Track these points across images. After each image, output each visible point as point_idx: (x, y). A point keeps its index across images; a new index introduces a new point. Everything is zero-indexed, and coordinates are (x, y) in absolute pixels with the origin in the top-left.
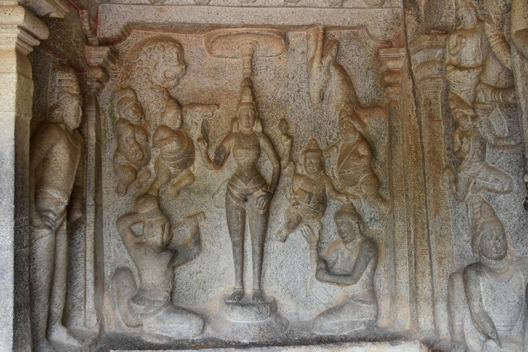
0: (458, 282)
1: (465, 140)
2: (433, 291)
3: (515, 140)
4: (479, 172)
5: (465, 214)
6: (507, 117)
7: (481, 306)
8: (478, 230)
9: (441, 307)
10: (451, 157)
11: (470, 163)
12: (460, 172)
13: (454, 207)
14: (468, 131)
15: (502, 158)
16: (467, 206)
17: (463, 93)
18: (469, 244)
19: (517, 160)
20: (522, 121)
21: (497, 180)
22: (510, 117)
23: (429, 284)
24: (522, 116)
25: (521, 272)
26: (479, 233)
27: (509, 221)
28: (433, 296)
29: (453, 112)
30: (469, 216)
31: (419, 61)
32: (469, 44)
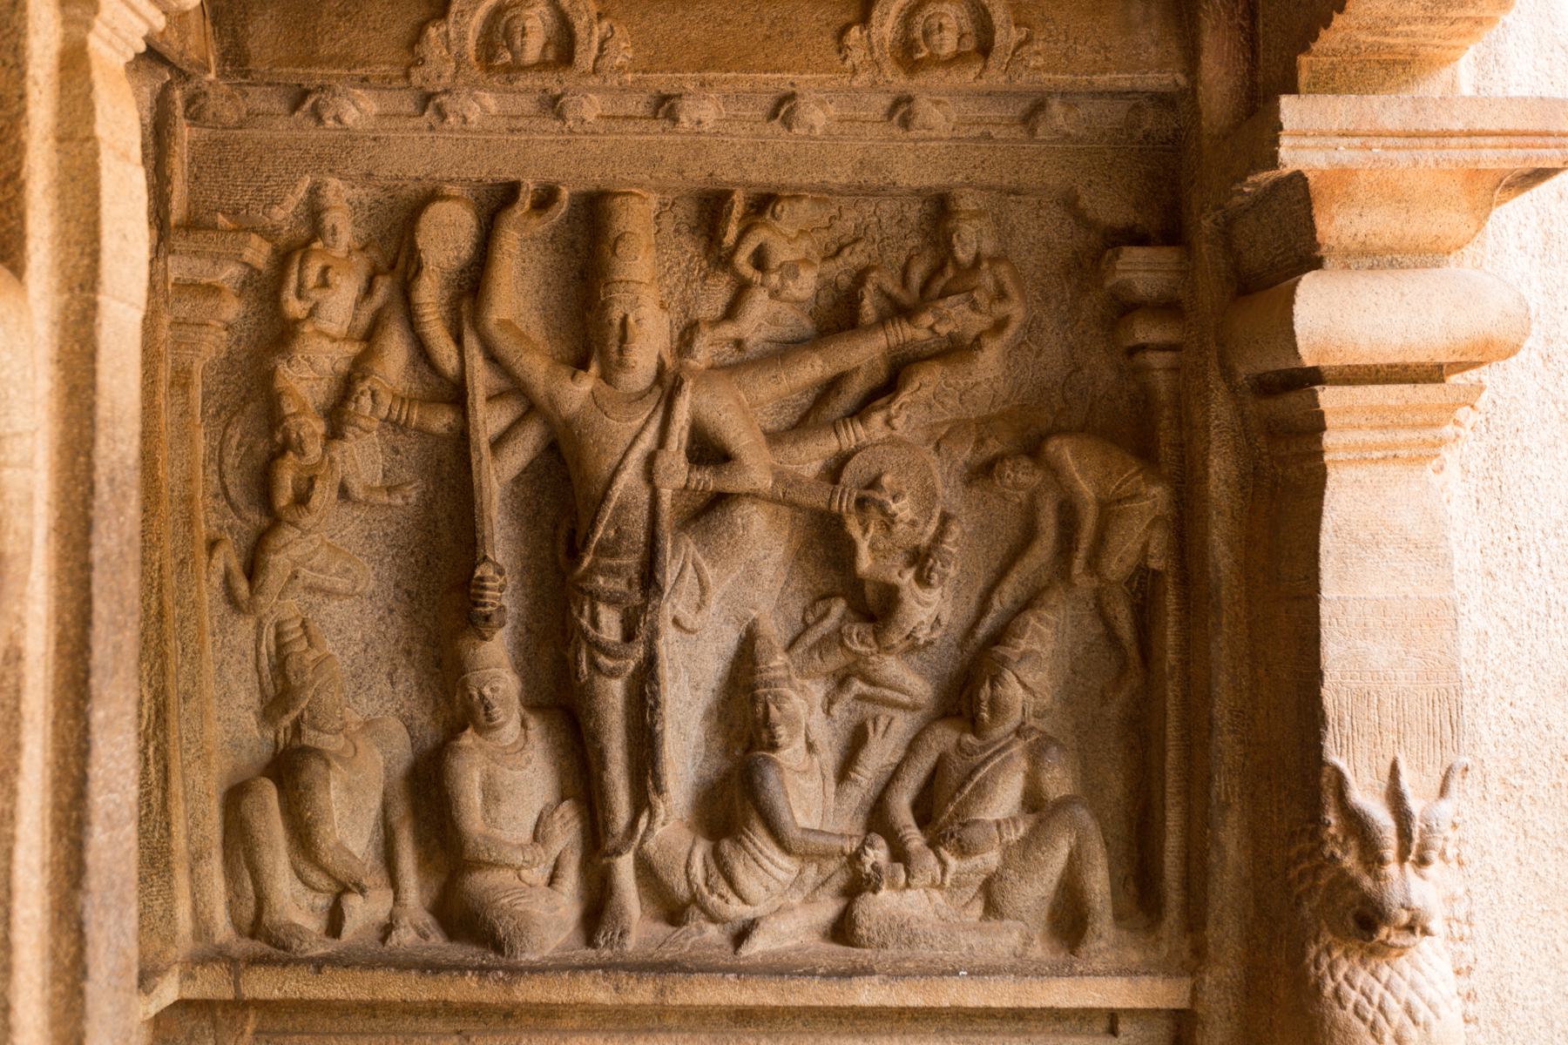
0: (269, 794)
1: (318, 485)
2: (189, 838)
3: (404, 497)
4: (316, 552)
5: (249, 646)
6: (388, 451)
7: (333, 830)
8: (310, 676)
9: (214, 867)
10: (224, 517)
11: (305, 533)
12: (276, 552)
13: (223, 631)
14: (320, 464)
15: (351, 528)
16: (259, 625)
17: (304, 383)
18: (250, 713)
19: (386, 534)
20: (479, 472)
21: (348, 570)
22: (397, 452)
23: (182, 821)
24: (480, 461)
25: (377, 751)
26: (312, 682)
27: (342, 654)
28: (189, 852)
29: (292, 420)
30: (263, 650)
31: (172, 276)
32: (343, 291)
